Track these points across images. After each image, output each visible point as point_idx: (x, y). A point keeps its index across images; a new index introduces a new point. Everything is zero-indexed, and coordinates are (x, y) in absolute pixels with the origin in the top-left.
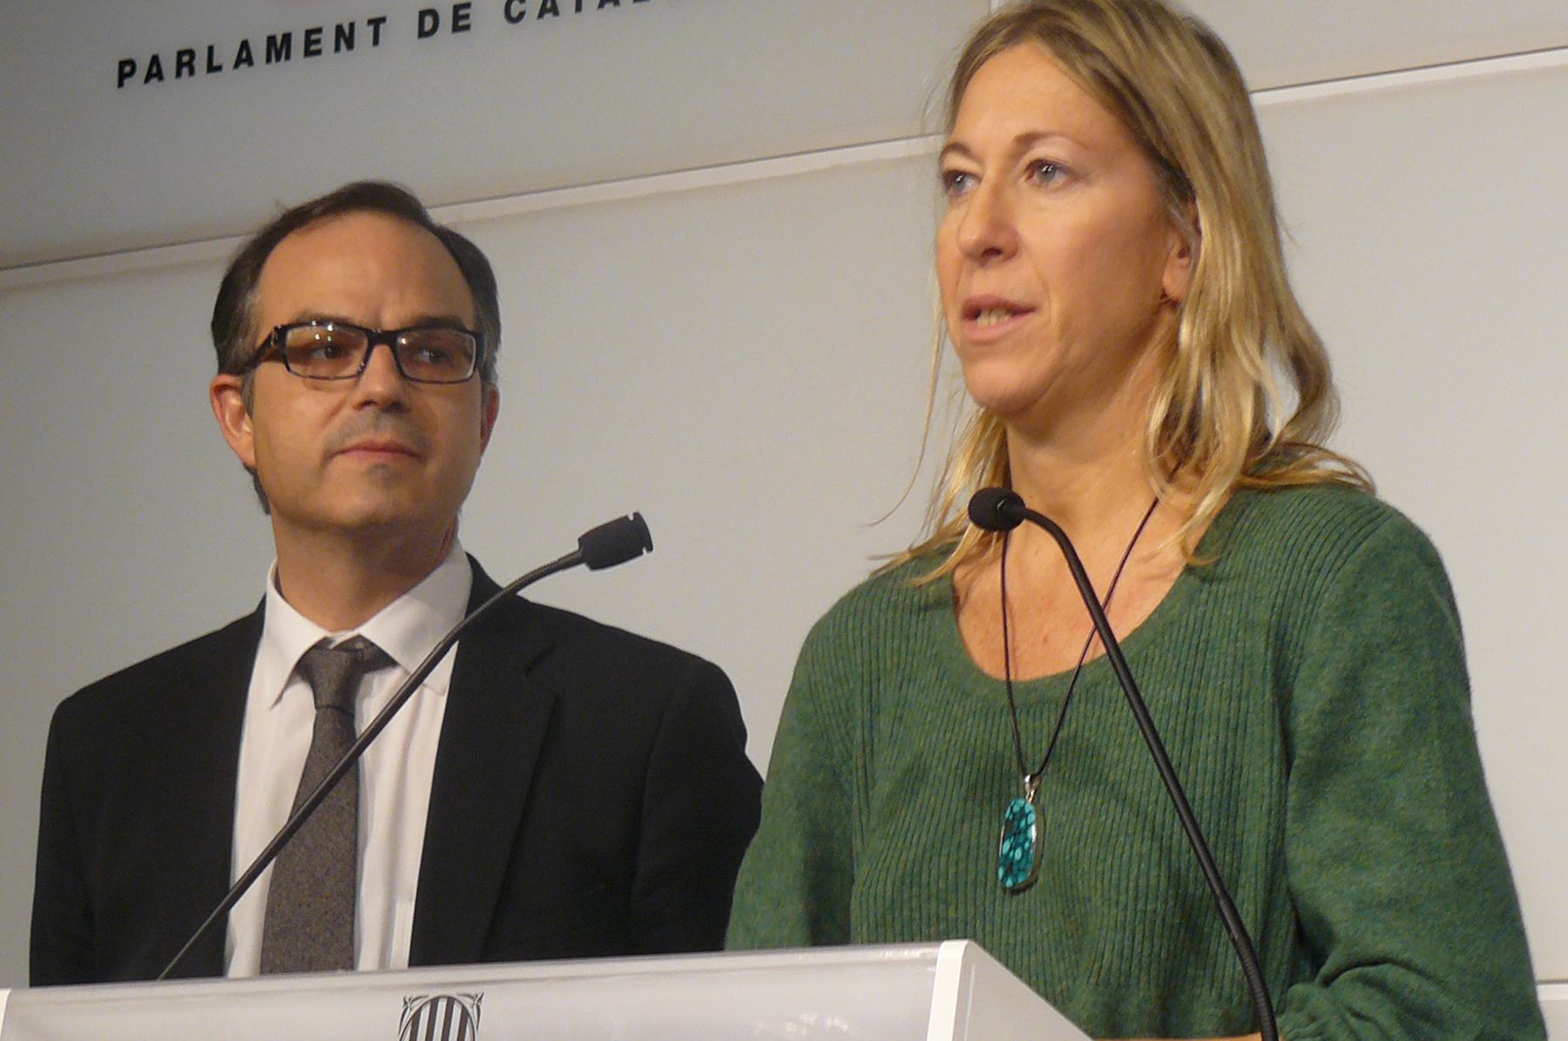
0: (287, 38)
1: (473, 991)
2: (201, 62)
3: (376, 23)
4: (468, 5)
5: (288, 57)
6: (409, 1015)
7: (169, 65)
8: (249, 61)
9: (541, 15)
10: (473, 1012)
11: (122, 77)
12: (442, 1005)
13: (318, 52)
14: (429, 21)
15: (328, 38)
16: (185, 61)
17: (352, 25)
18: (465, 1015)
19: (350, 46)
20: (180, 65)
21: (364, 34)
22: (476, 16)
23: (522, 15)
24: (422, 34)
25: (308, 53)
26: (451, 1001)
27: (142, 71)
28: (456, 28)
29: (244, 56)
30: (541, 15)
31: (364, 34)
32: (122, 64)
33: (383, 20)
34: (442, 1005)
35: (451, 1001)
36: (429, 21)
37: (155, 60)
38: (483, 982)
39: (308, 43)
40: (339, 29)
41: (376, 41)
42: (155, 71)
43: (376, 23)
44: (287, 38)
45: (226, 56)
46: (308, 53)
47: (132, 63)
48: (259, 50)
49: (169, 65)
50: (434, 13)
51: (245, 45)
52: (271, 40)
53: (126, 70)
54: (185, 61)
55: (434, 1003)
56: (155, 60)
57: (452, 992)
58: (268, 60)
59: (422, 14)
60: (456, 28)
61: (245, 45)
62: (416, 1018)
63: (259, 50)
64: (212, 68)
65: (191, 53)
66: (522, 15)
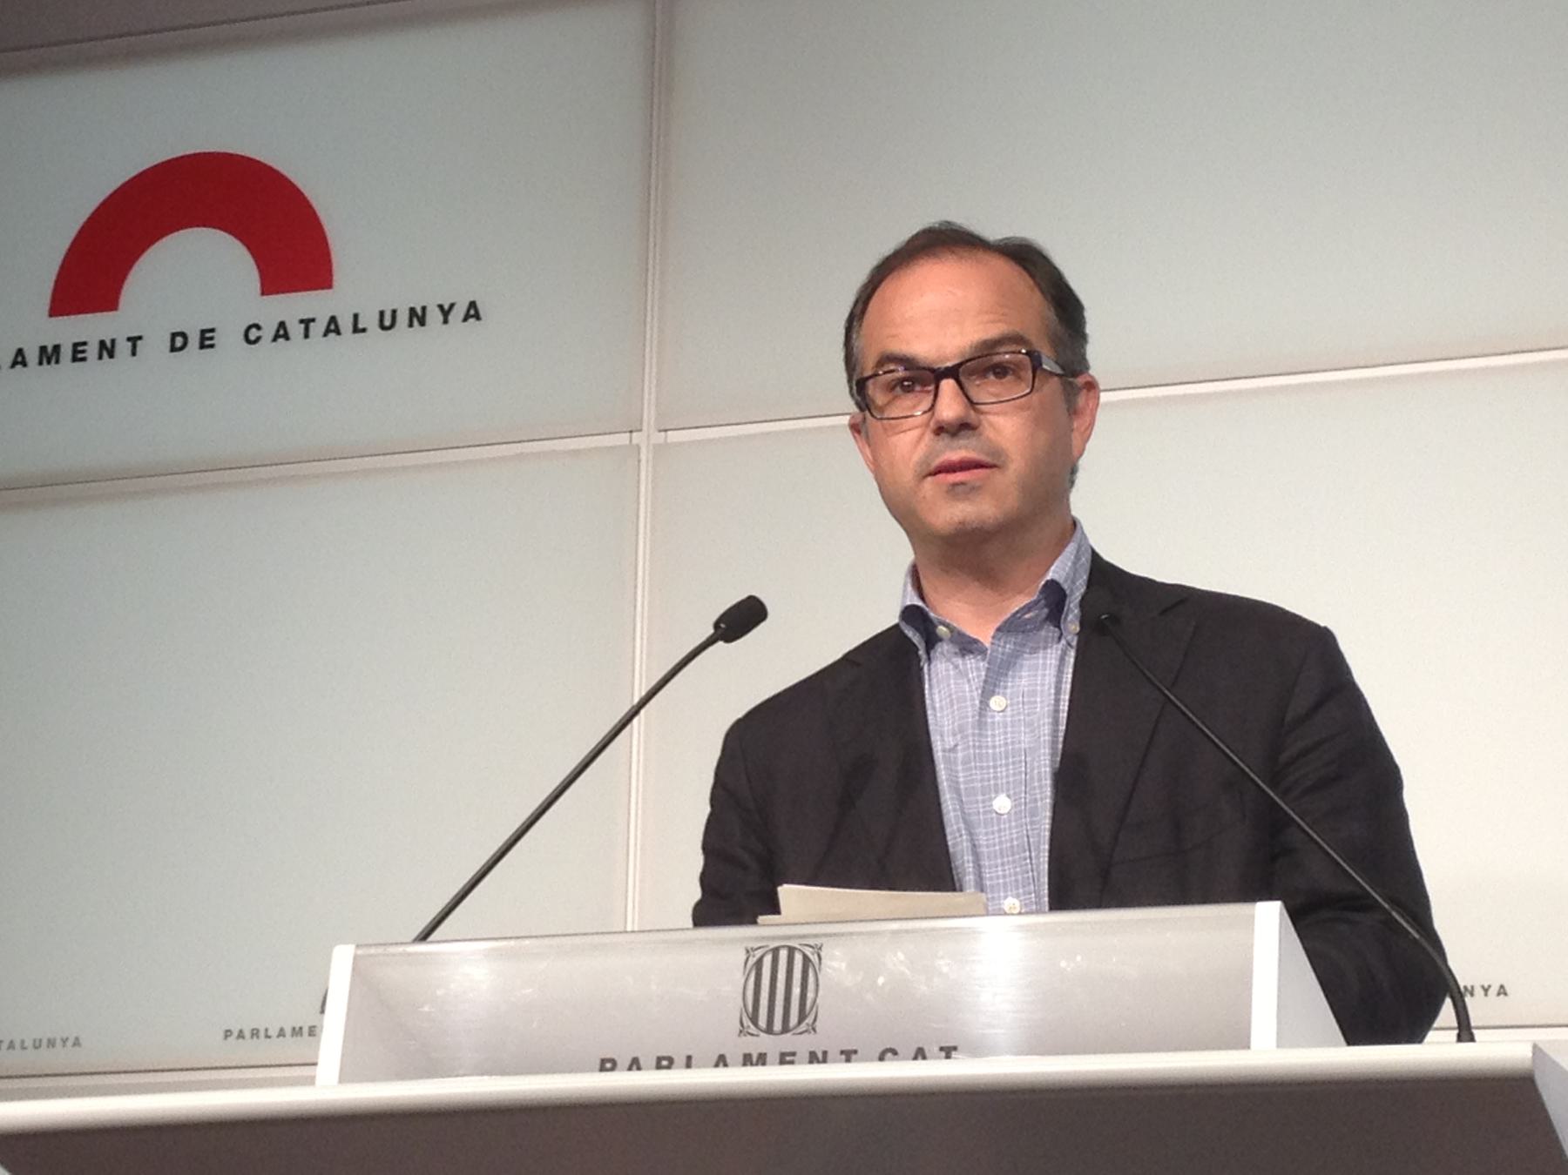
0: (57, 348)
1: (818, 942)
3: (134, 340)
4: (212, 330)
5: (57, 362)
6: (752, 961)
9: (275, 340)
10: (814, 958)
12: (783, 954)
13: (84, 359)
14: (179, 341)
15: (92, 350)
17: (113, 341)
18: (806, 959)
19: (111, 355)
21: (123, 348)
22: (219, 339)
23: (258, 339)
24: (173, 349)
25: (75, 359)
26: (791, 950)
28: (202, 347)
30: (275, 340)
31: (123, 348)
33: (140, 338)
34: (783, 954)
35: (791, 950)
36: (179, 341)
38: (826, 935)
40: (102, 343)
41: (134, 354)
43: (134, 340)
44: (57, 348)
46: (75, 359)
48: (32, 356)
50: (183, 335)
51: (20, 352)
52: (43, 349)
55: (775, 951)
58: (41, 363)
59: (174, 335)
61: (20, 352)
62: (759, 964)
63: (32, 356)
66: (258, 339)
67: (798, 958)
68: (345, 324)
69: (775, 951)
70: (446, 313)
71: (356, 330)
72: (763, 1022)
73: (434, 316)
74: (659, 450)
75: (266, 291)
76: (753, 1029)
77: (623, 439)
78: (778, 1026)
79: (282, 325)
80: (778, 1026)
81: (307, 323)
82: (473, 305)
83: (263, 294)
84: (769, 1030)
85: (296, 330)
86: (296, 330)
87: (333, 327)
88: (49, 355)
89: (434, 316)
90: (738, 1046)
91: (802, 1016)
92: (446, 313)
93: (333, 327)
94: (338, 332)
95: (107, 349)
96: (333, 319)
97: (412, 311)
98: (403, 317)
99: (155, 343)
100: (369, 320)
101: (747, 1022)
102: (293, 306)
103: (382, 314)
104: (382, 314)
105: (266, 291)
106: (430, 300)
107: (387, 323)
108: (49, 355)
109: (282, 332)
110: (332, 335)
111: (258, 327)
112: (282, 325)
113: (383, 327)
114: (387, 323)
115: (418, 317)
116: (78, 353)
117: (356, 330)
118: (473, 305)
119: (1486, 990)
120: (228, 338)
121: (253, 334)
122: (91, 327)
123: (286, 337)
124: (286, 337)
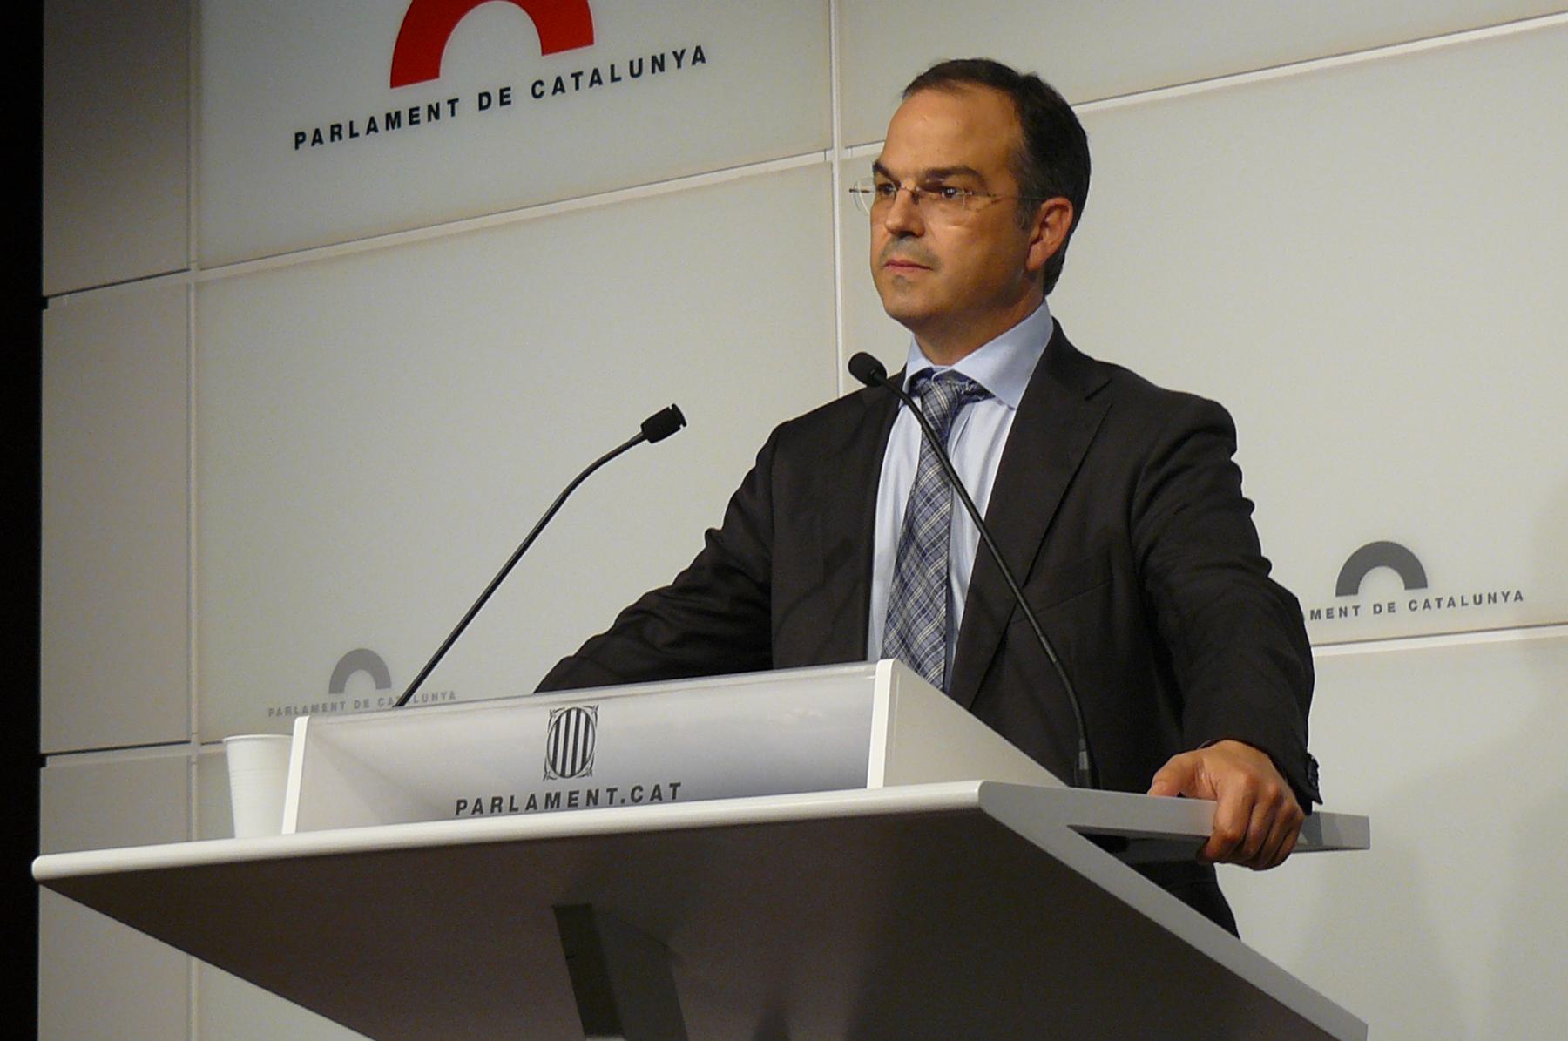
0: (398, 114)
2: (345, 132)
3: (452, 102)
7: (326, 134)
8: (376, 130)
10: (592, 717)
11: (298, 143)
12: (574, 713)
14: (485, 100)
16: (336, 131)
18: (588, 719)
19: (437, 117)
20: (333, 134)
21: (445, 109)
22: (513, 96)
24: (481, 107)
25: (411, 123)
27: (310, 137)
28: (502, 103)
29: (372, 127)
31: (445, 109)
32: (297, 135)
34: (574, 713)
35: (579, 711)
36: (485, 100)
37: (317, 131)
39: (411, 116)
40: (430, 107)
41: (453, 114)
42: (317, 139)
43: (452, 102)
44: (398, 114)
45: (361, 127)
46: (411, 123)
47: (303, 134)
48: (381, 122)
49: (326, 134)
50: (488, 95)
51: (372, 120)
52: (388, 116)
53: (299, 138)
54: (336, 131)
55: (569, 712)
56: (317, 131)
57: (579, 706)
59: (481, 96)
60: (502, 103)
61: (372, 120)
62: (558, 722)
63: (381, 122)
64: (353, 135)
65: (339, 126)
67: (583, 717)
68: (605, 75)
69: (569, 712)
70: (679, 58)
71: (614, 79)
72: (559, 768)
73: (670, 62)
74: (844, 164)
75: (546, 50)
76: (552, 774)
77: (818, 158)
78: (568, 772)
79: (559, 80)
80: (568, 772)
81: (576, 76)
82: (698, 49)
83: (544, 52)
84: (563, 775)
85: (569, 83)
86: (569, 83)
87: (596, 79)
88: (393, 120)
89: (670, 62)
90: (542, 789)
91: (584, 763)
92: (679, 58)
93: (596, 79)
94: (599, 82)
95: (434, 112)
96: (596, 72)
97: (654, 58)
98: (647, 64)
99: (469, 104)
100: (623, 71)
101: (549, 769)
102: (567, 62)
103: (632, 63)
104: (632, 63)
105: (546, 50)
106: (667, 49)
107: (636, 71)
108: (393, 120)
109: (559, 86)
110: (596, 85)
111: (541, 83)
112: (559, 80)
113: (633, 75)
114: (636, 71)
115: (658, 64)
116: (413, 113)
117: (614, 79)
118: (698, 49)
119: (1506, 596)
120: (521, 94)
121: (538, 89)
122: (419, 94)
123: (563, 90)
124: (563, 90)
